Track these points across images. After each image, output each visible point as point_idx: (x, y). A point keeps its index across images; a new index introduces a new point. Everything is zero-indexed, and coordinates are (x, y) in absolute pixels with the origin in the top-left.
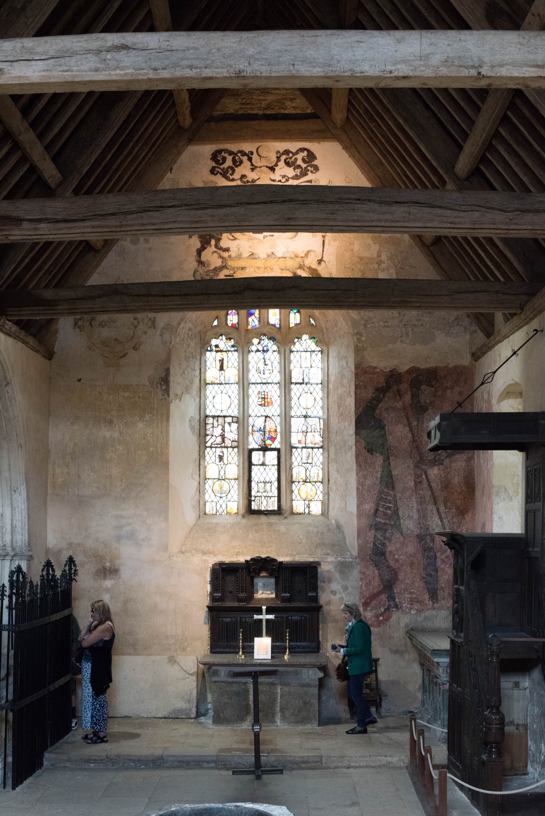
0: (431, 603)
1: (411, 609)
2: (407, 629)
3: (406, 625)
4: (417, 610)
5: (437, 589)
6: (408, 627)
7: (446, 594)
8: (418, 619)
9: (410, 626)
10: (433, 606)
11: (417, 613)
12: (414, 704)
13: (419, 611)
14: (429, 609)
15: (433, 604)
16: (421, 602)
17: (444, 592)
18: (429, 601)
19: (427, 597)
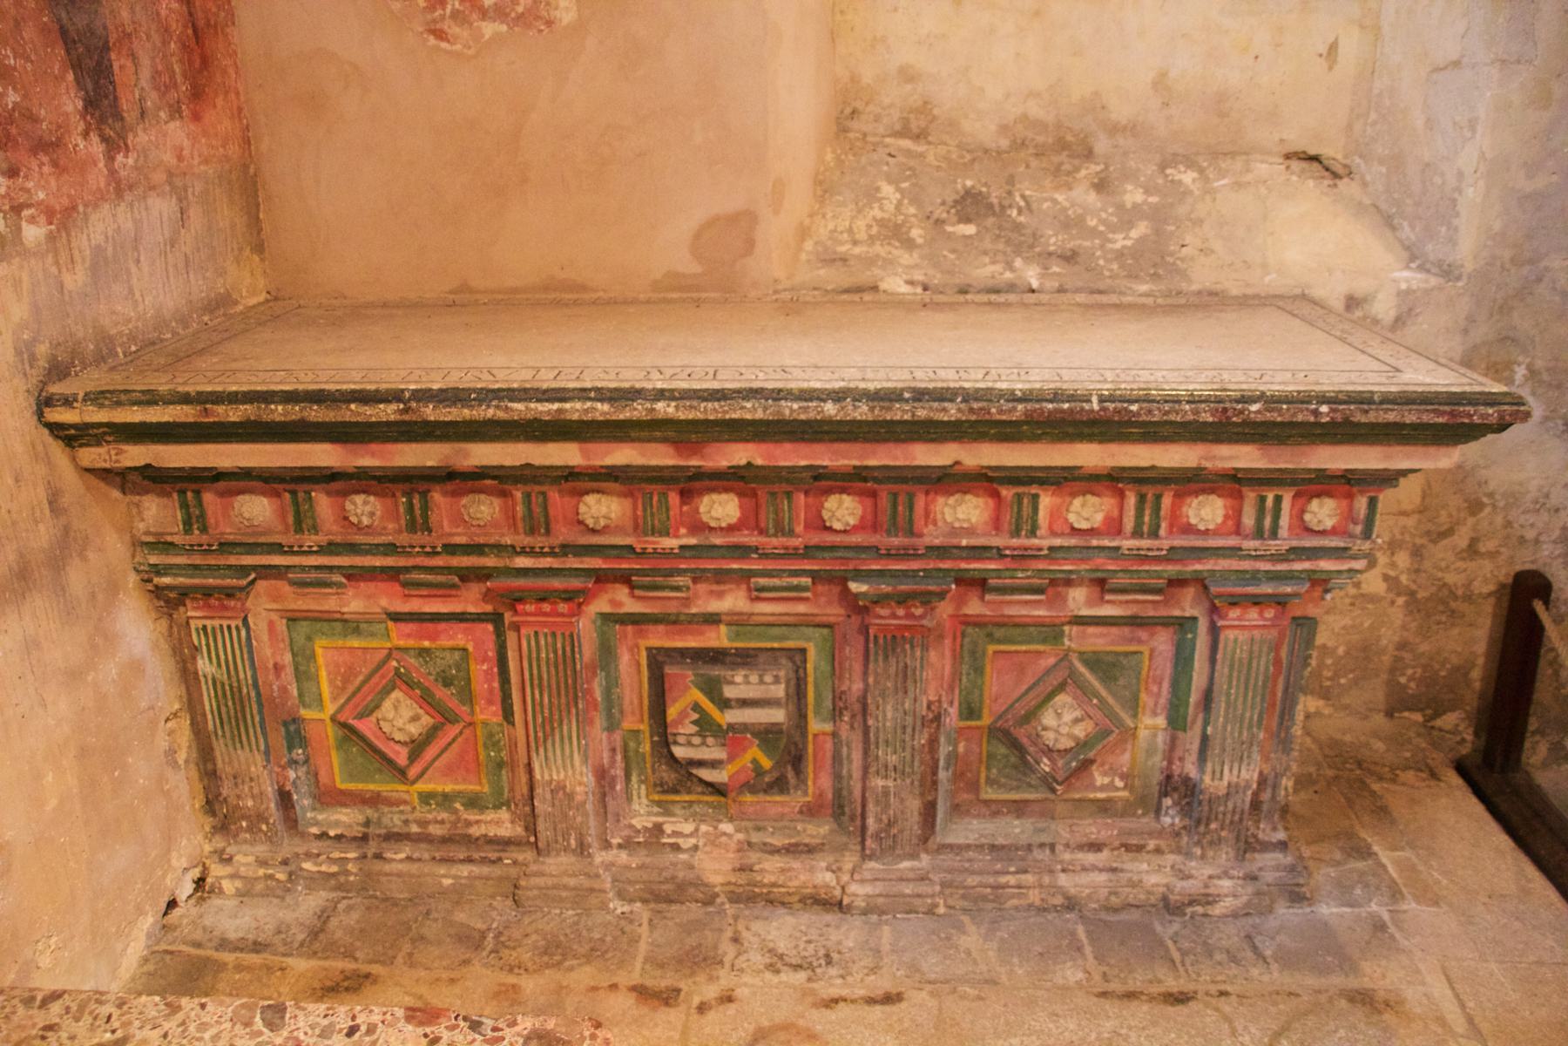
0: (97, 147)
1: (17, 209)
2: (35, 375)
3: (18, 353)
4: (50, 214)
5: (106, 48)
6: (33, 358)
7: (146, 74)
8: (68, 279)
9: (43, 349)
10: (112, 172)
11: (51, 238)
12: (174, 862)
13: (63, 218)
14: (101, 197)
15: (110, 159)
16: (49, 146)
17: (133, 56)
18: (86, 134)
19: (71, 104)
